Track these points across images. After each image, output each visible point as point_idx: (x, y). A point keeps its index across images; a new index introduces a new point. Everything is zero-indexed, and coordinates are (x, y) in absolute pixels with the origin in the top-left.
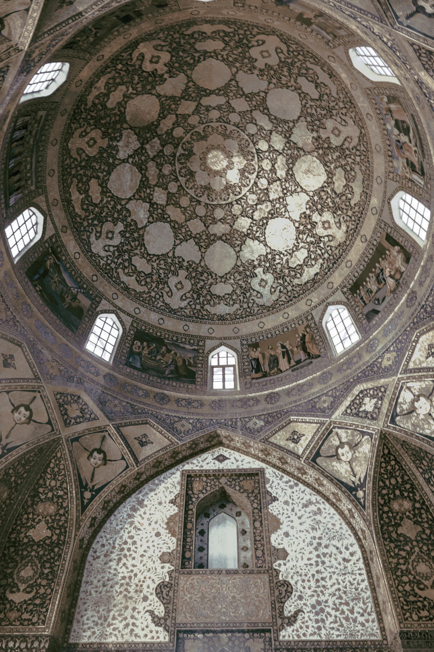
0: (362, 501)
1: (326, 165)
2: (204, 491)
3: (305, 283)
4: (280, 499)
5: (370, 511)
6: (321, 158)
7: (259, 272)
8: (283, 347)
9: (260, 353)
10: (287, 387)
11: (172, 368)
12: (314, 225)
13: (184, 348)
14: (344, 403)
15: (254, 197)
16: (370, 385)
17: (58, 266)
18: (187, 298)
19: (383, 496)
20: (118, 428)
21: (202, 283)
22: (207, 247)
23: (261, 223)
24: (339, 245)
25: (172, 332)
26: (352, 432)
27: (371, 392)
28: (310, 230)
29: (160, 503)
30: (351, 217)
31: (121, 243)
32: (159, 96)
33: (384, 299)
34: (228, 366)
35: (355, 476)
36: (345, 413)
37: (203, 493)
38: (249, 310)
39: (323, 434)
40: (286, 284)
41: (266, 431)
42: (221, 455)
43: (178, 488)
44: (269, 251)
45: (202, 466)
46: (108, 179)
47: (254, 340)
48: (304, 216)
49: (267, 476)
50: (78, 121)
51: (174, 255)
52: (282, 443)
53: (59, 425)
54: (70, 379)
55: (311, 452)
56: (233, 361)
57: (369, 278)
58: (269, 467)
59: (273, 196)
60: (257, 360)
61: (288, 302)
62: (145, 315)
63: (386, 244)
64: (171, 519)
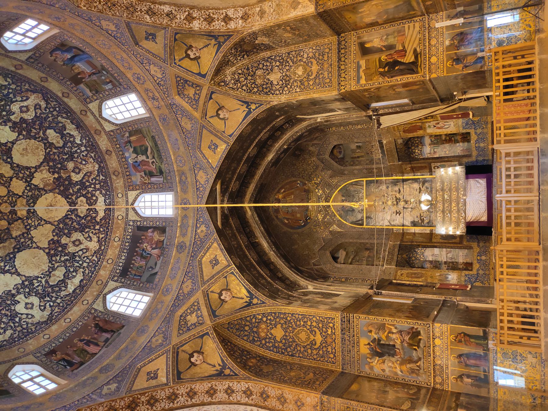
0: (232, 373)
1: (68, 198)
3: (73, 291)
5: (243, 372)
6: (62, 193)
8: (81, 341)
9: (62, 354)
10: (112, 357)
12: (65, 246)
16: (184, 308)
24: (95, 253)
27: (189, 311)
28: (61, 251)
33: (156, 264)
36: (179, 335)
39: (173, 357)
40: (53, 299)
47: (47, 350)
55: (173, 375)
57: (134, 260)
60: (64, 359)
61: (64, 310)
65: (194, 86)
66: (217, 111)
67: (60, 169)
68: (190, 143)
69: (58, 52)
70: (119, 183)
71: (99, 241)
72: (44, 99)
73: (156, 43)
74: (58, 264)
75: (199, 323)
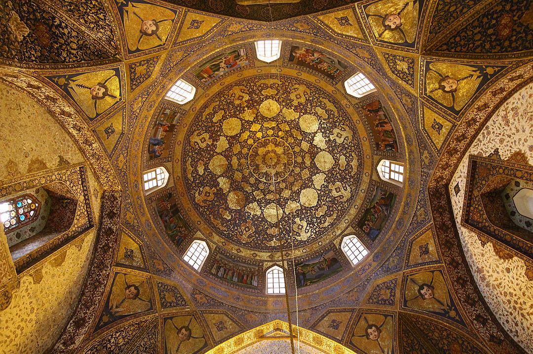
0: (497, 69)
2: (482, 213)
4: (497, 146)
6: (259, 103)
7: (333, 138)
8: (377, 126)
9: (382, 143)
11: (384, 208)
13: (375, 196)
14: (404, 86)
15: (289, 139)
16: (386, 66)
17: (305, 265)
18: (345, 187)
19: (492, 47)
20: (408, 266)
21: (338, 175)
22: (317, 168)
23: (304, 135)
25: (364, 201)
26: (428, 79)
29: (483, 255)
30: (289, 83)
31: (306, 221)
32: (229, 192)
34: (390, 167)
35: (472, 76)
36: (412, 85)
37: (483, 214)
38: (356, 146)
41: (432, 150)
42: (455, 188)
43: (473, 234)
44: (319, 131)
45: (460, 207)
46: (270, 222)
47: (374, 146)
48: (296, 110)
49: (476, 153)
50: (232, 236)
51: (319, 190)
52: (442, 139)
53: (389, 308)
54: (364, 287)
55: (450, 115)
56: (387, 162)
57: (321, 68)
58: (469, 150)
59: (288, 129)
61: (349, 120)
62: (350, 217)
63: (295, 60)
64: (497, 252)
65: (133, 70)
66: (150, 35)
67: (241, 107)
68: (197, 46)
69: (157, 154)
70: (249, 73)
71: (298, 84)
72: (192, 134)
73: (112, 124)
74: (313, 110)
75: (411, 63)
